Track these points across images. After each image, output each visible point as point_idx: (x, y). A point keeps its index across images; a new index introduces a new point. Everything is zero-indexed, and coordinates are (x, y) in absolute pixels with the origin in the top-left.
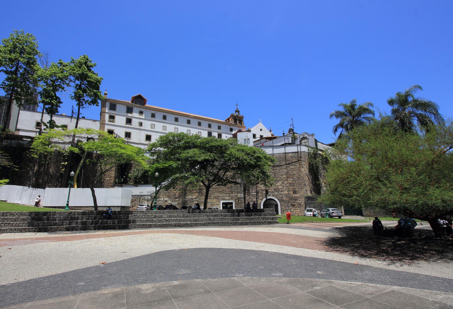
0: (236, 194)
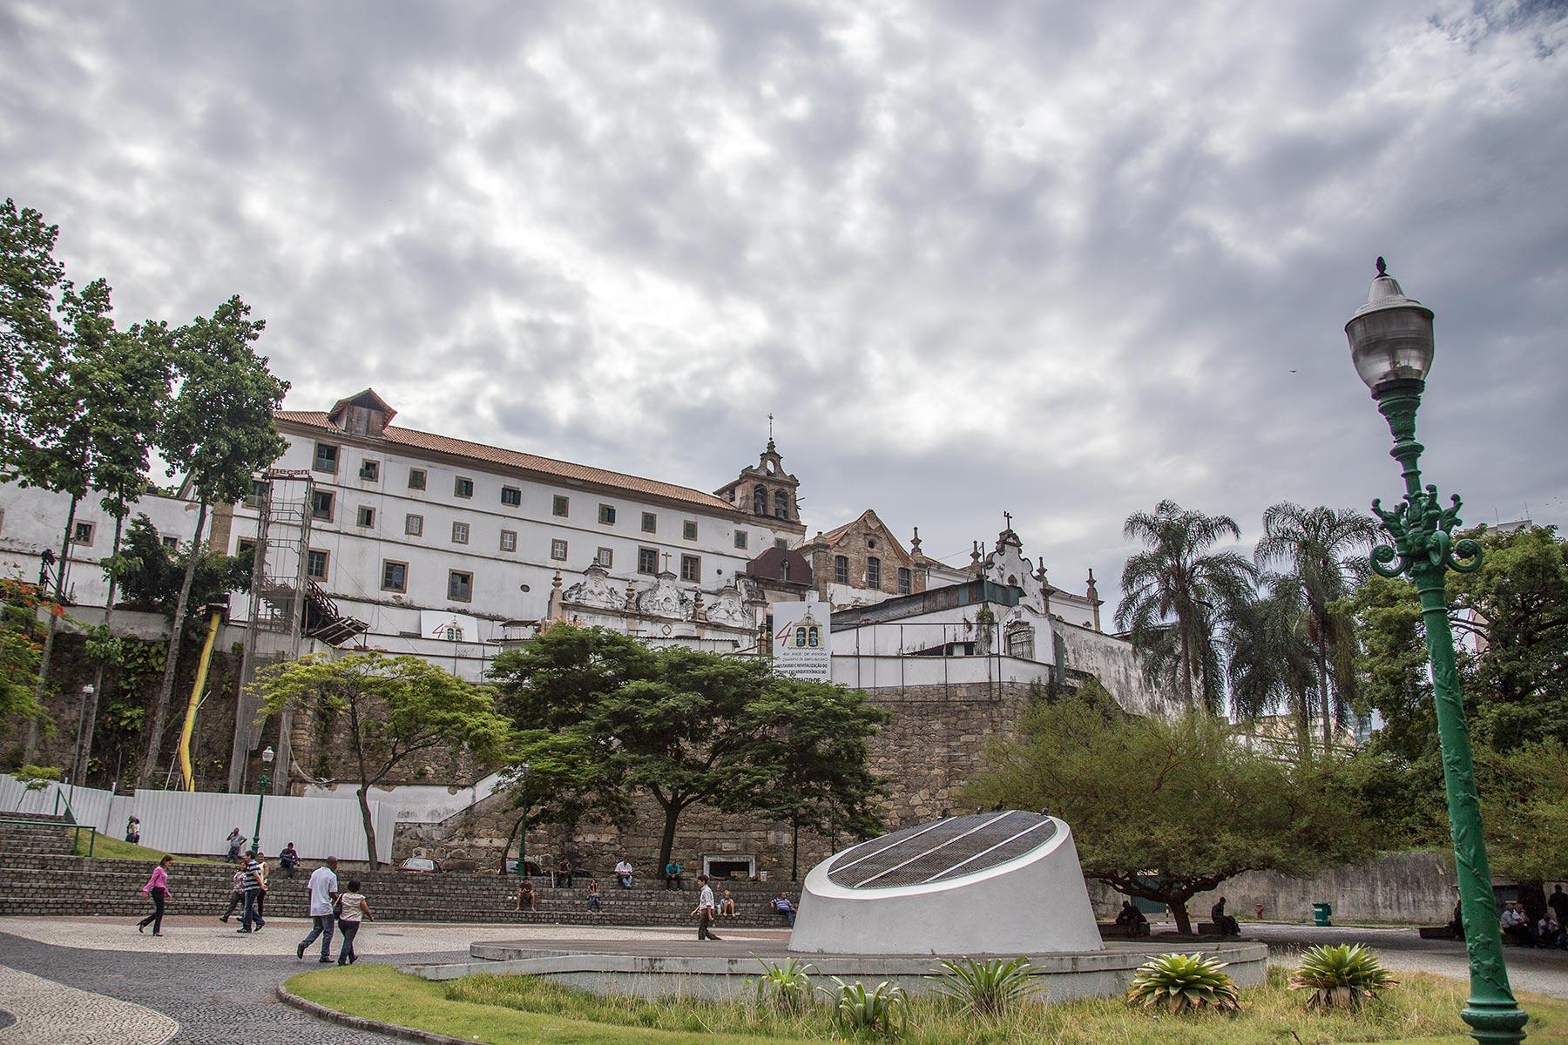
0: (763, 834)
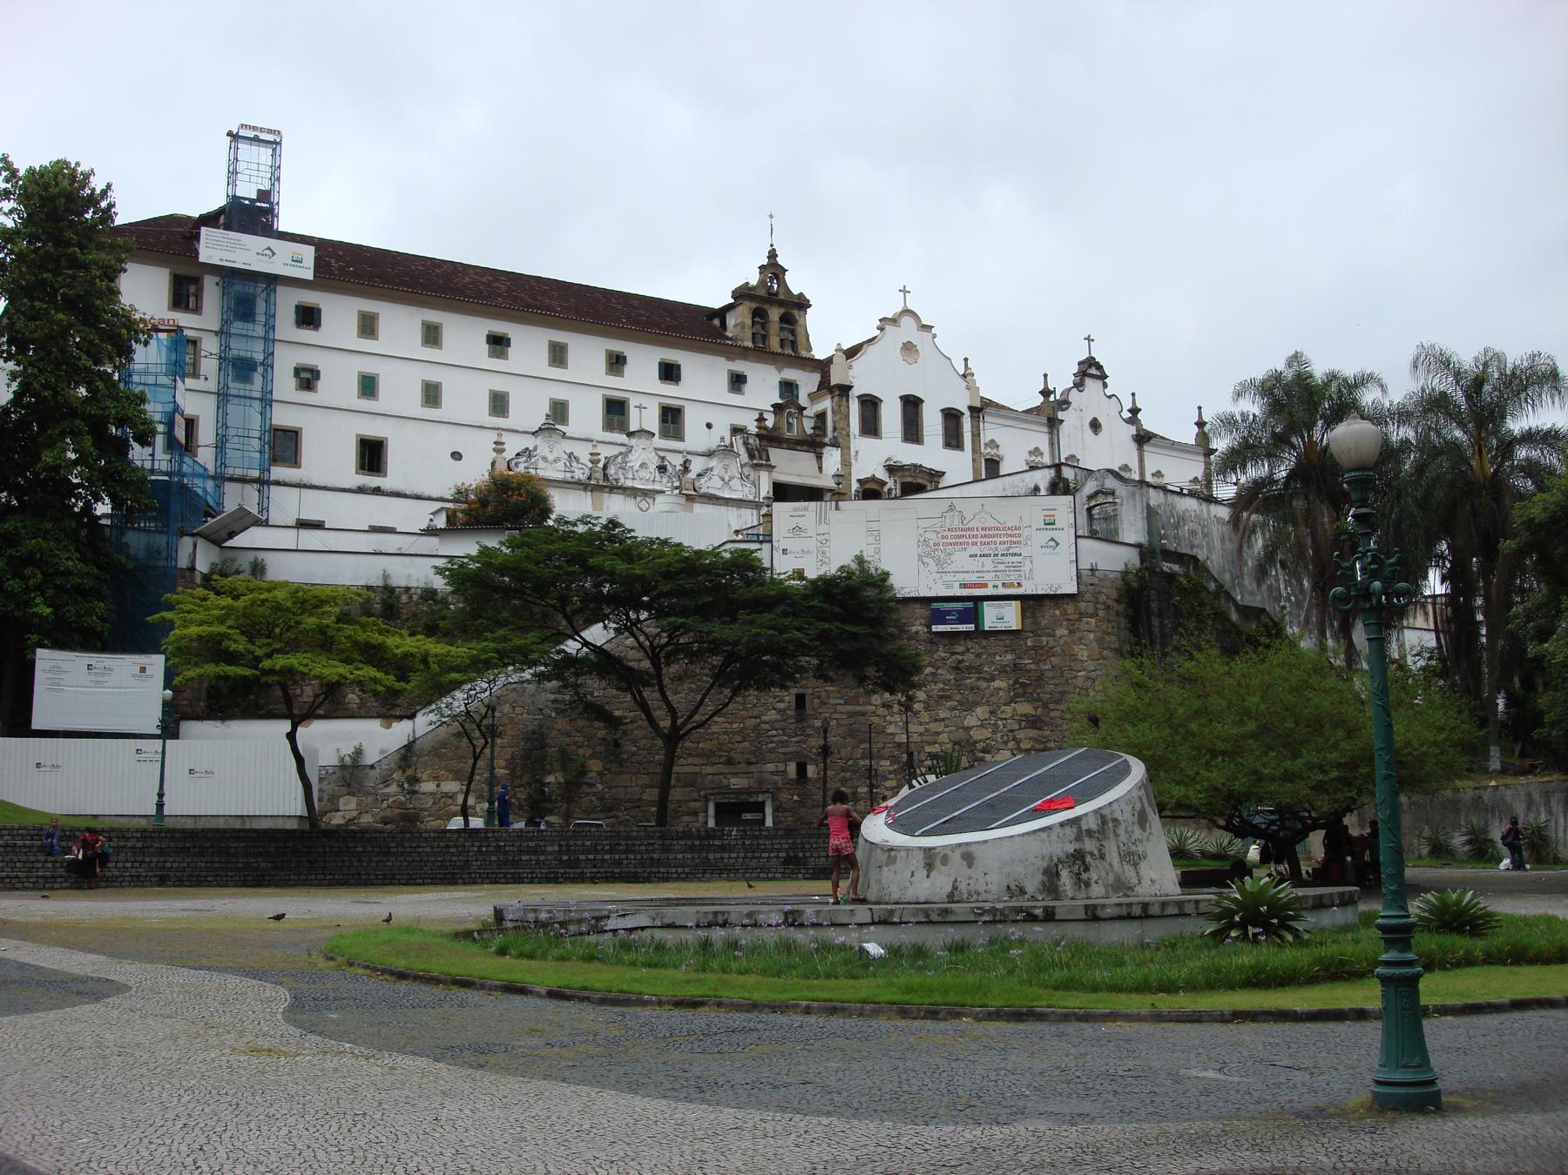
0: (781, 767)
